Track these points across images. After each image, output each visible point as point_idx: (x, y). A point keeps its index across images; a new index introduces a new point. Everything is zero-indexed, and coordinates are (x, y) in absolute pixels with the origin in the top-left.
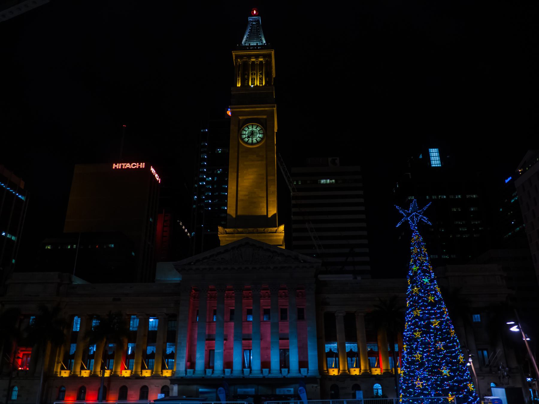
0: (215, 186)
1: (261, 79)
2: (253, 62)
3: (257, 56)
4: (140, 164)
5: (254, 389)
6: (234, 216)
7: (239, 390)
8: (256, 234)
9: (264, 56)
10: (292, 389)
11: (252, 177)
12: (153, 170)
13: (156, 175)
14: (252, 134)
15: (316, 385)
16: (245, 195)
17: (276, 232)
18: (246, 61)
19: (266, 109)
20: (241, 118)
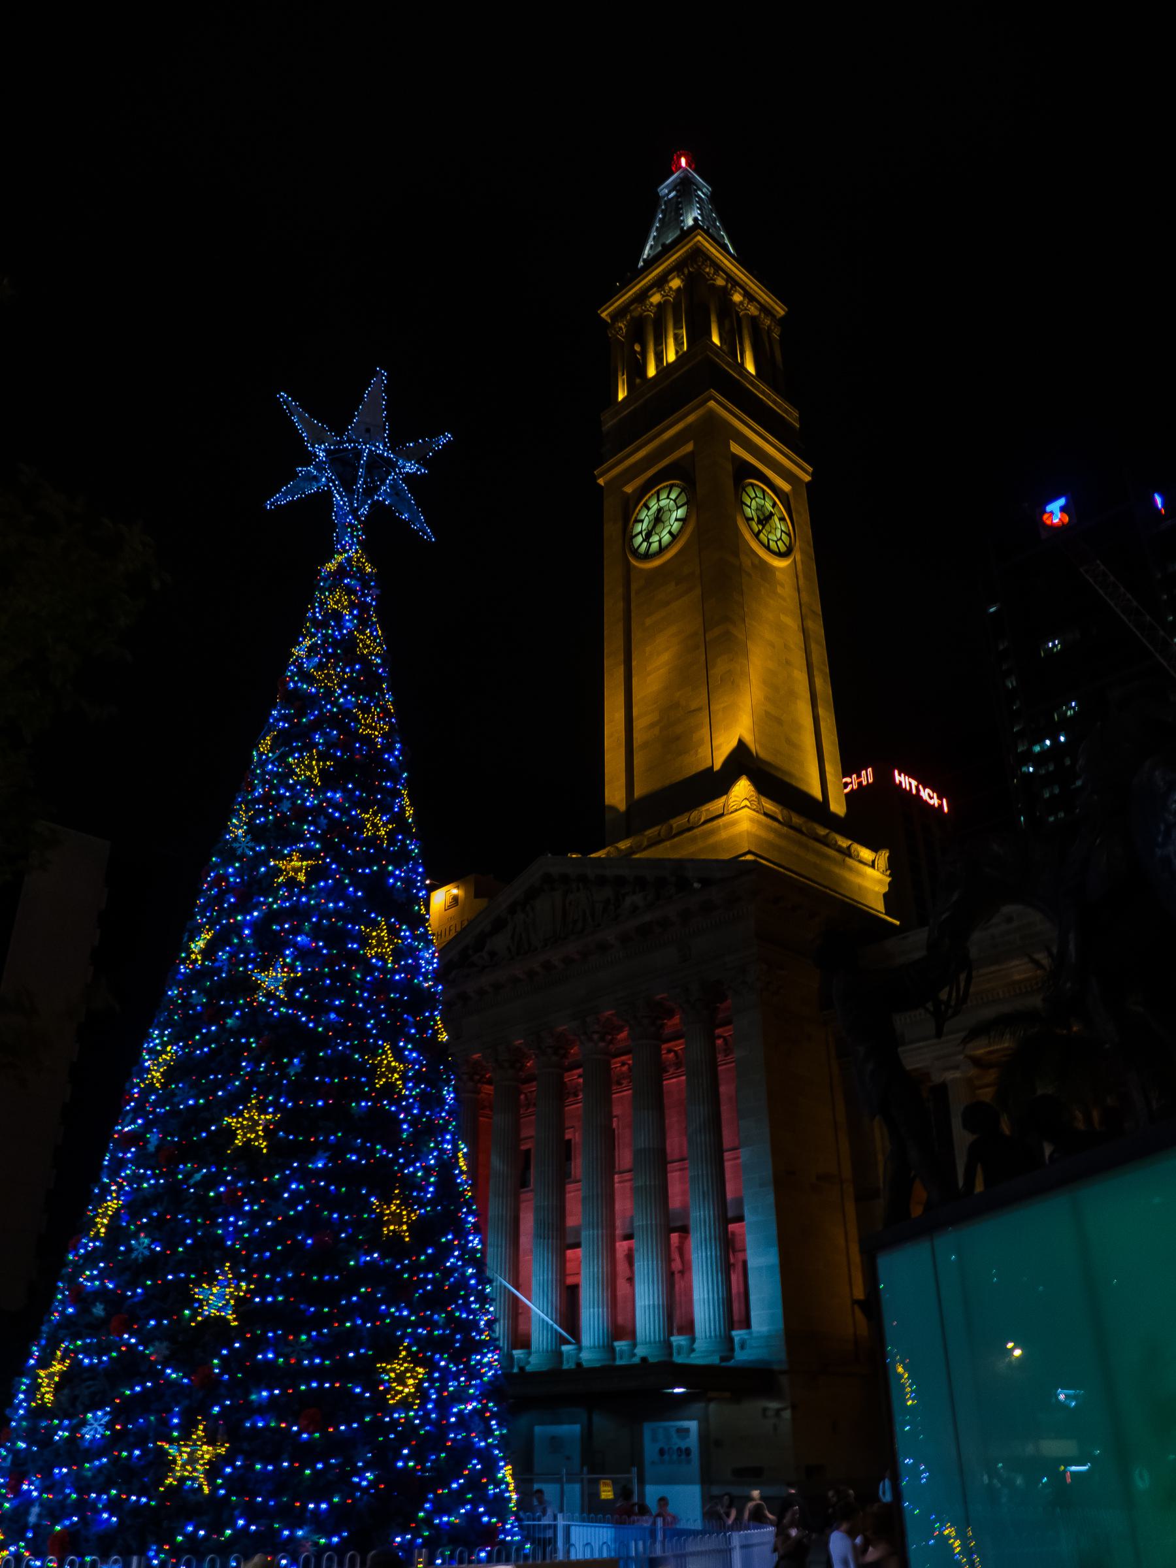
0: (1068, 762)
1: (678, 342)
2: (659, 305)
4: (859, 776)
5: (576, 1428)
6: (622, 807)
8: (668, 843)
9: (677, 268)
10: (693, 1425)
11: (665, 657)
13: (925, 794)
14: (658, 519)
15: (774, 1405)
16: (652, 725)
17: (722, 815)
18: (641, 315)
19: (691, 419)
20: (629, 489)
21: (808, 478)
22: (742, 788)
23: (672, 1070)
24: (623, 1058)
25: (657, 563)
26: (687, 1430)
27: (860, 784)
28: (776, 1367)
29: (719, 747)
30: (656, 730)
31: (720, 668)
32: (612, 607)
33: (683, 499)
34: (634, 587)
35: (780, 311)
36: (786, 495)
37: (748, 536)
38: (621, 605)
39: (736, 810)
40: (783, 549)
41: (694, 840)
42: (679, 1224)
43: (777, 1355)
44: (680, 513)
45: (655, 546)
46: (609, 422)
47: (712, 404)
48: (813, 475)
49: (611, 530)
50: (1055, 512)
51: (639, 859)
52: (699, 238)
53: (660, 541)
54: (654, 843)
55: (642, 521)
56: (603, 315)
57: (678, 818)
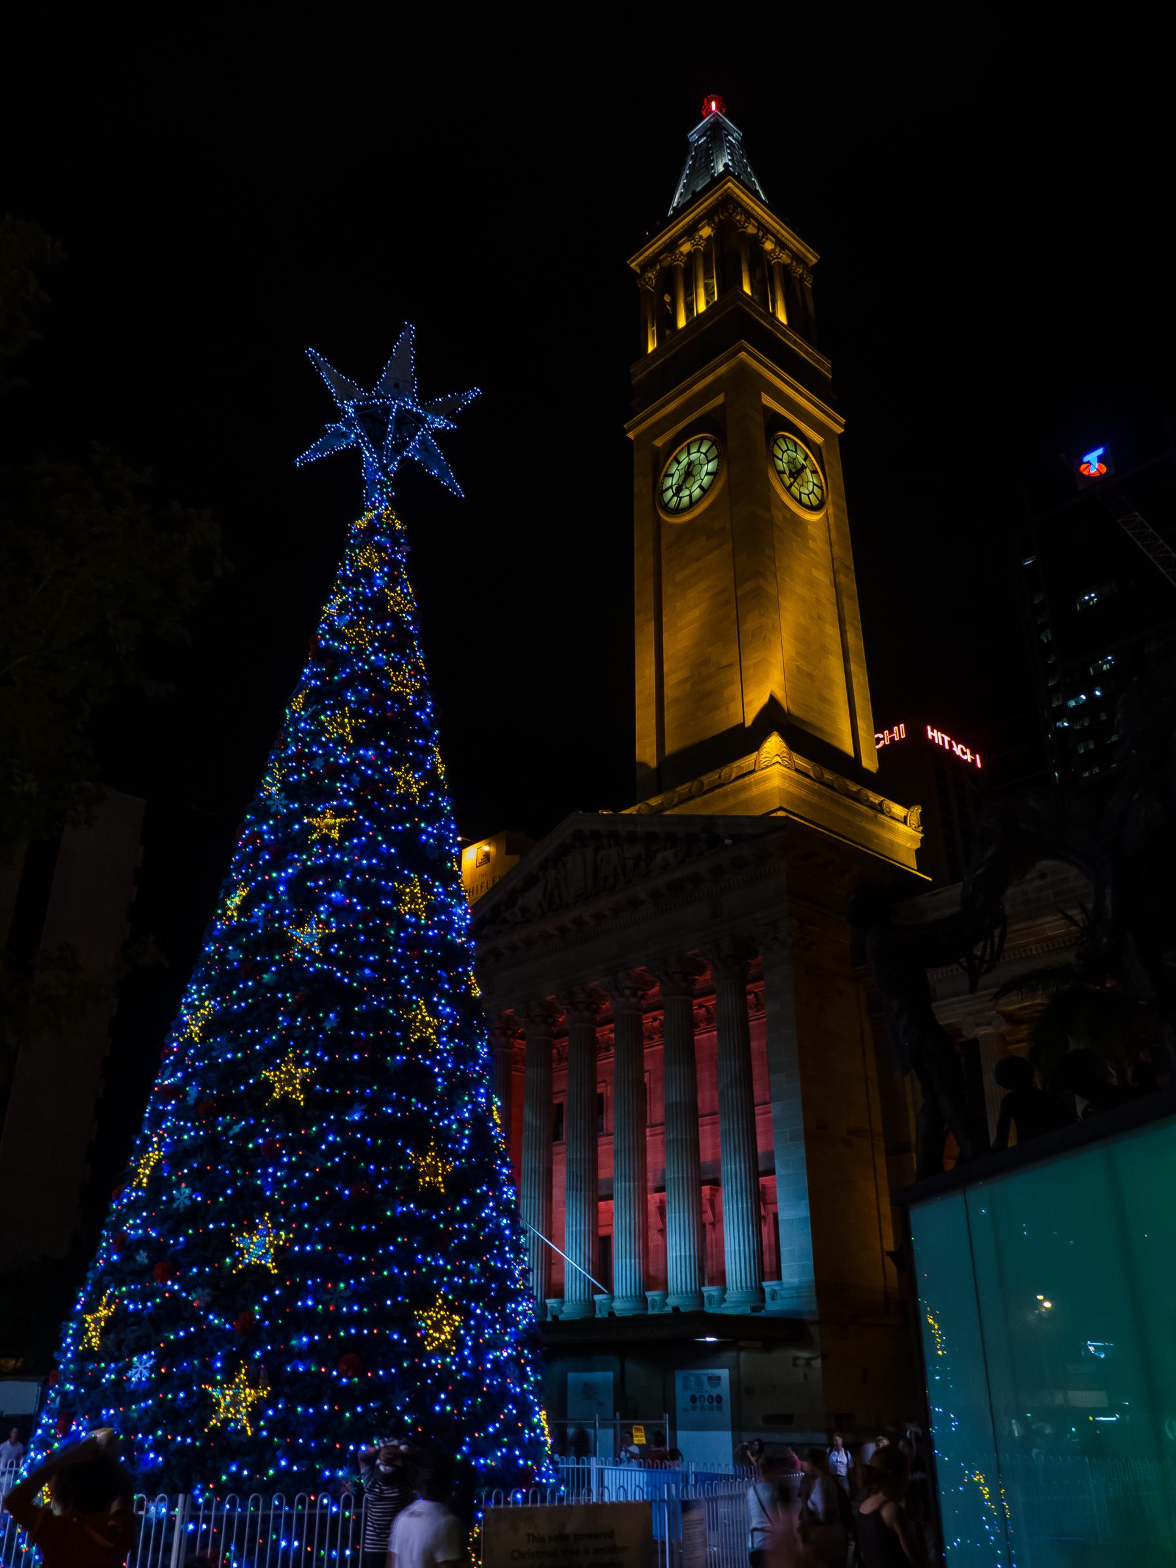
0: (1103, 717)
1: (708, 289)
3: (691, 231)
4: (891, 732)
5: (610, 1375)
6: (653, 764)
7: (571, 1376)
8: (698, 800)
9: (708, 216)
10: (724, 1373)
11: (696, 613)
12: (937, 736)
13: (958, 749)
14: (689, 473)
15: (804, 1354)
16: (684, 681)
17: (753, 771)
19: (722, 370)
20: (659, 443)
21: (840, 430)
22: (774, 745)
23: (703, 1025)
24: (655, 1013)
25: (687, 518)
26: (719, 1378)
27: (892, 739)
28: (806, 1318)
29: (751, 702)
30: (688, 686)
31: (750, 624)
32: (642, 564)
33: (714, 452)
34: (665, 541)
35: (813, 258)
36: (819, 447)
37: (779, 490)
38: (651, 560)
39: (768, 766)
40: (815, 502)
41: (725, 796)
42: (710, 1177)
43: (807, 1305)
44: (711, 467)
45: (686, 500)
46: (639, 375)
47: (743, 355)
48: (845, 426)
49: (641, 485)
50: (1093, 463)
51: (670, 816)
52: (730, 184)
53: (690, 495)
54: (684, 800)
55: (672, 475)
56: (633, 265)
57: (709, 775)
